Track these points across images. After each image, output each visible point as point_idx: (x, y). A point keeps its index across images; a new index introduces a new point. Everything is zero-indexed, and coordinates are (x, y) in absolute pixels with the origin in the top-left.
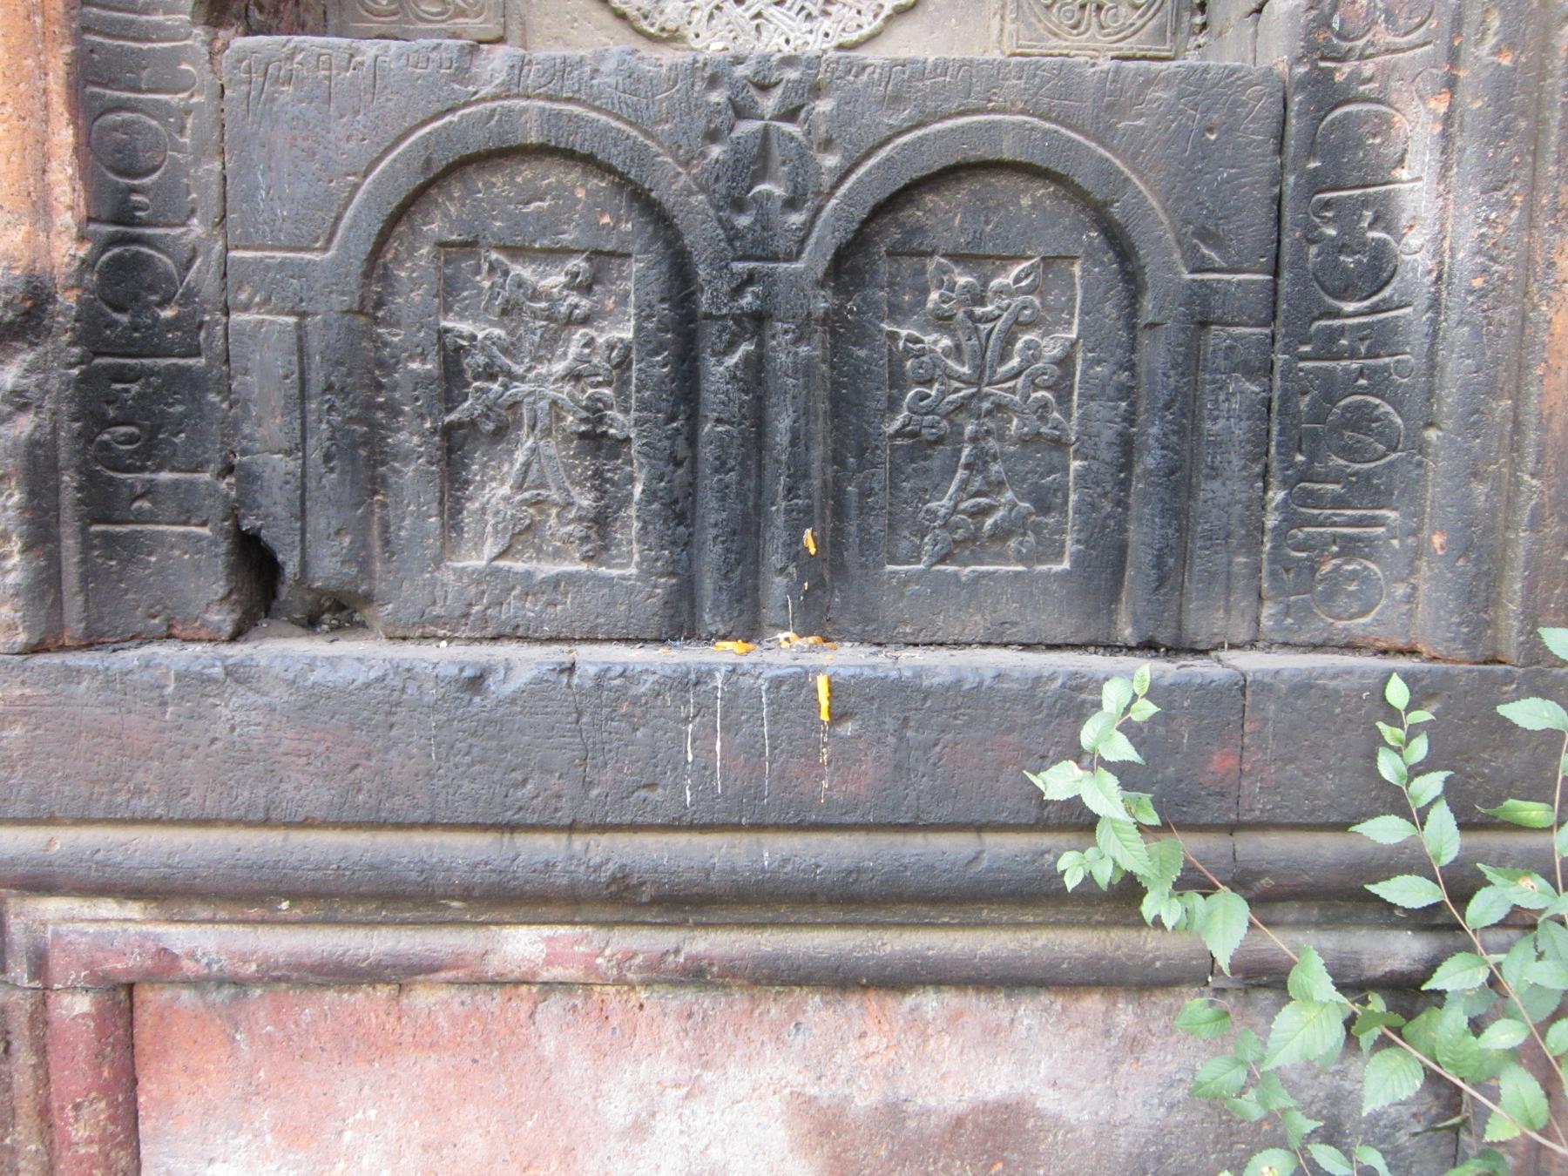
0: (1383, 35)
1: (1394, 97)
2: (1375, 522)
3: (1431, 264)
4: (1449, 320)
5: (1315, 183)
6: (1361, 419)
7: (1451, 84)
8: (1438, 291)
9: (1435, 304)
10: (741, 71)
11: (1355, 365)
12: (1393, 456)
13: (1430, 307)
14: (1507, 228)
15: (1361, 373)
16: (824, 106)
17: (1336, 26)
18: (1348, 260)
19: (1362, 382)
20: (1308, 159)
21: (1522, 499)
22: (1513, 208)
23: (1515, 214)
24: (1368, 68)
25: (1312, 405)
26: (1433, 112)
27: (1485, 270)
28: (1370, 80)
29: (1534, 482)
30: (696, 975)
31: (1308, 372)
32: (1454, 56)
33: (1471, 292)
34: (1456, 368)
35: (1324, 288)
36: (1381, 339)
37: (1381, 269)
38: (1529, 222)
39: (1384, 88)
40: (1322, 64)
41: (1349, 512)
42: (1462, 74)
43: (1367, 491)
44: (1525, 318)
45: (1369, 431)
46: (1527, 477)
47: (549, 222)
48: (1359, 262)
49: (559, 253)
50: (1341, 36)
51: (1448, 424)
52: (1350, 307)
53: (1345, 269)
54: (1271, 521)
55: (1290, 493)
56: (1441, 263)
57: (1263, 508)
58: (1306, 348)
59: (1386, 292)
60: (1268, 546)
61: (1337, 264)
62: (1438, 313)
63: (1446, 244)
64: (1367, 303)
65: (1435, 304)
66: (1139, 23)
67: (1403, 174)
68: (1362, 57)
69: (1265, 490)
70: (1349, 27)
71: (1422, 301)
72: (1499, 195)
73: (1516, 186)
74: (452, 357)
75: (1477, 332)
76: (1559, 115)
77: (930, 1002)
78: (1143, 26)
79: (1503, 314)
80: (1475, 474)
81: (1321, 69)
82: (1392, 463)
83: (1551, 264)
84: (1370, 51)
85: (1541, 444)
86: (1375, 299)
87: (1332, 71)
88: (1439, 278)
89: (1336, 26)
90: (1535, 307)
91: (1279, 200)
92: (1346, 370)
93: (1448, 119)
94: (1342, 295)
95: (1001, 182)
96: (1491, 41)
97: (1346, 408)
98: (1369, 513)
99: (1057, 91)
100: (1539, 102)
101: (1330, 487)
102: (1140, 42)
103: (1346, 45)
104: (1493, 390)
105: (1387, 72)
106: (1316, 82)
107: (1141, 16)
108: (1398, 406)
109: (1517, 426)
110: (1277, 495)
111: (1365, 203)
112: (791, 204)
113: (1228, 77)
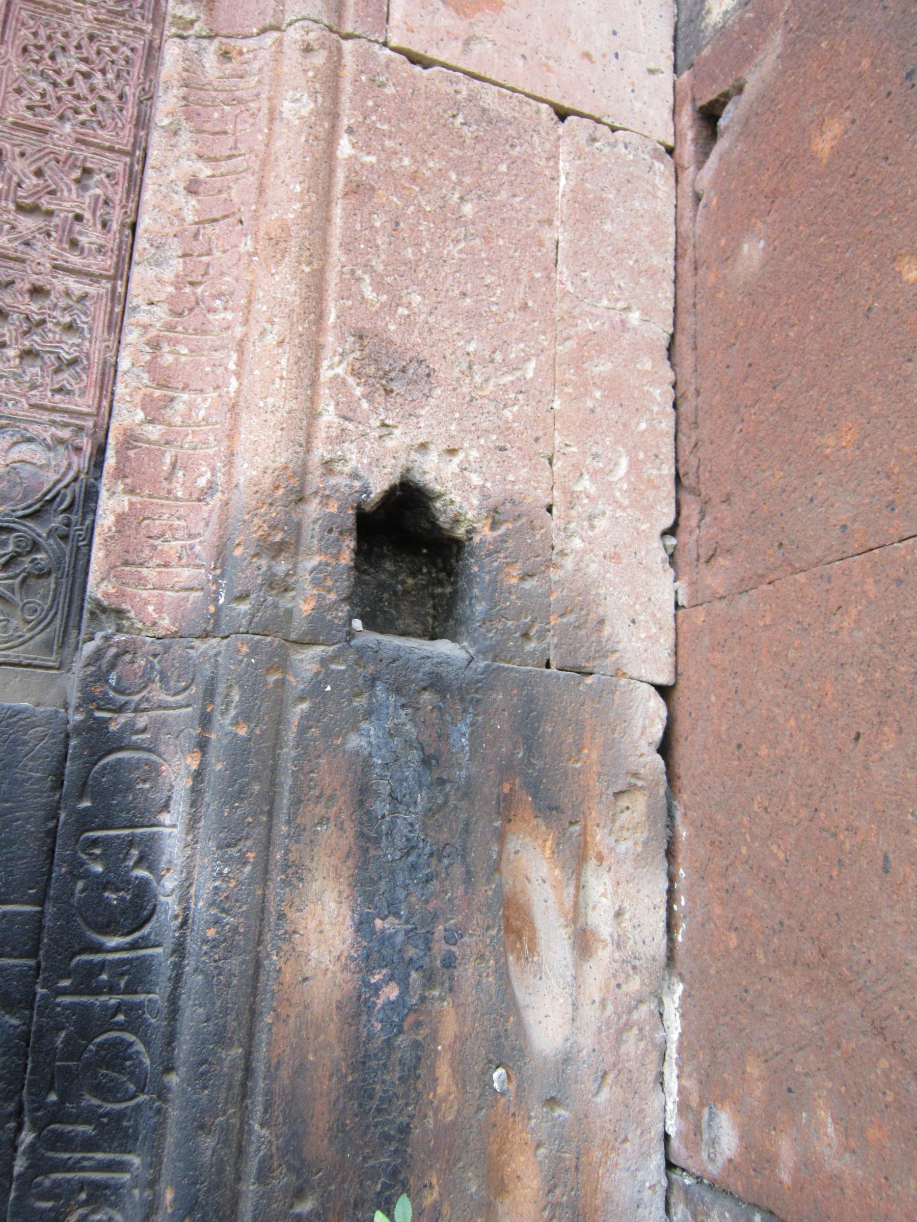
0: (157, 694)
1: (162, 748)
2: (121, 1167)
3: (177, 909)
4: (190, 965)
5: (85, 821)
6: (117, 1055)
7: (202, 745)
8: (183, 936)
9: (180, 949)
11: (114, 1000)
12: (142, 1098)
13: (174, 952)
14: (239, 883)
15: (118, 1009)
17: (113, 682)
18: (112, 896)
19: (121, 1017)
20: (81, 797)
21: (253, 1148)
22: (245, 864)
23: (247, 869)
24: (142, 721)
25: (66, 1042)
26: (187, 767)
27: (217, 922)
28: (144, 730)
29: (264, 1132)
31: (66, 1007)
32: (206, 720)
33: (205, 941)
34: (192, 1014)
35: (88, 923)
36: (137, 975)
37: (143, 908)
38: (264, 873)
39: (155, 739)
40: (98, 714)
41: (100, 1156)
42: (213, 736)
43: (116, 1133)
44: (258, 965)
45: (122, 1070)
46: (257, 1127)
48: (122, 899)
50: (115, 689)
51: (182, 1070)
52: (113, 941)
53: (109, 905)
54: (19, 1165)
55: (38, 1137)
56: (186, 909)
57: (15, 1149)
58: (65, 983)
59: (145, 930)
60: (12, 1195)
61: (101, 900)
62: (183, 958)
63: (192, 891)
64: (129, 939)
65: (180, 949)
66: (28, 635)
67: (166, 818)
68: (136, 710)
69: (19, 1129)
70: (125, 684)
71: (169, 944)
72: (233, 851)
73: (249, 843)
75: (208, 983)
76: (290, 782)
78: (31, 638)
79: (234, 964)
80: (202, 1127)
81: (97, 719)
82: (138, 1106)
83: (282, 916)
84: (145, 705)
85: (269, 1093)
86: (137, 935)
87: (107, 721)
88: (184, 923)
89: (113, 682)
90: (268, 956)
91: (52, 834)
92: (104, 1006)
93: (198, 775)
94: (107, 928)
96: (233, 712)
97: (101, 1045)
98: (117, 1157)
100: (274, 769)
101: (81, 1128)
102: (26, 651)
103: (122, 699)
104: (222, 1039)
106: (90, 729)
107: (31, 630)
108: (147, 1044)
109: (248, 1071)
110: (27, 1137)
113: (10, 717)
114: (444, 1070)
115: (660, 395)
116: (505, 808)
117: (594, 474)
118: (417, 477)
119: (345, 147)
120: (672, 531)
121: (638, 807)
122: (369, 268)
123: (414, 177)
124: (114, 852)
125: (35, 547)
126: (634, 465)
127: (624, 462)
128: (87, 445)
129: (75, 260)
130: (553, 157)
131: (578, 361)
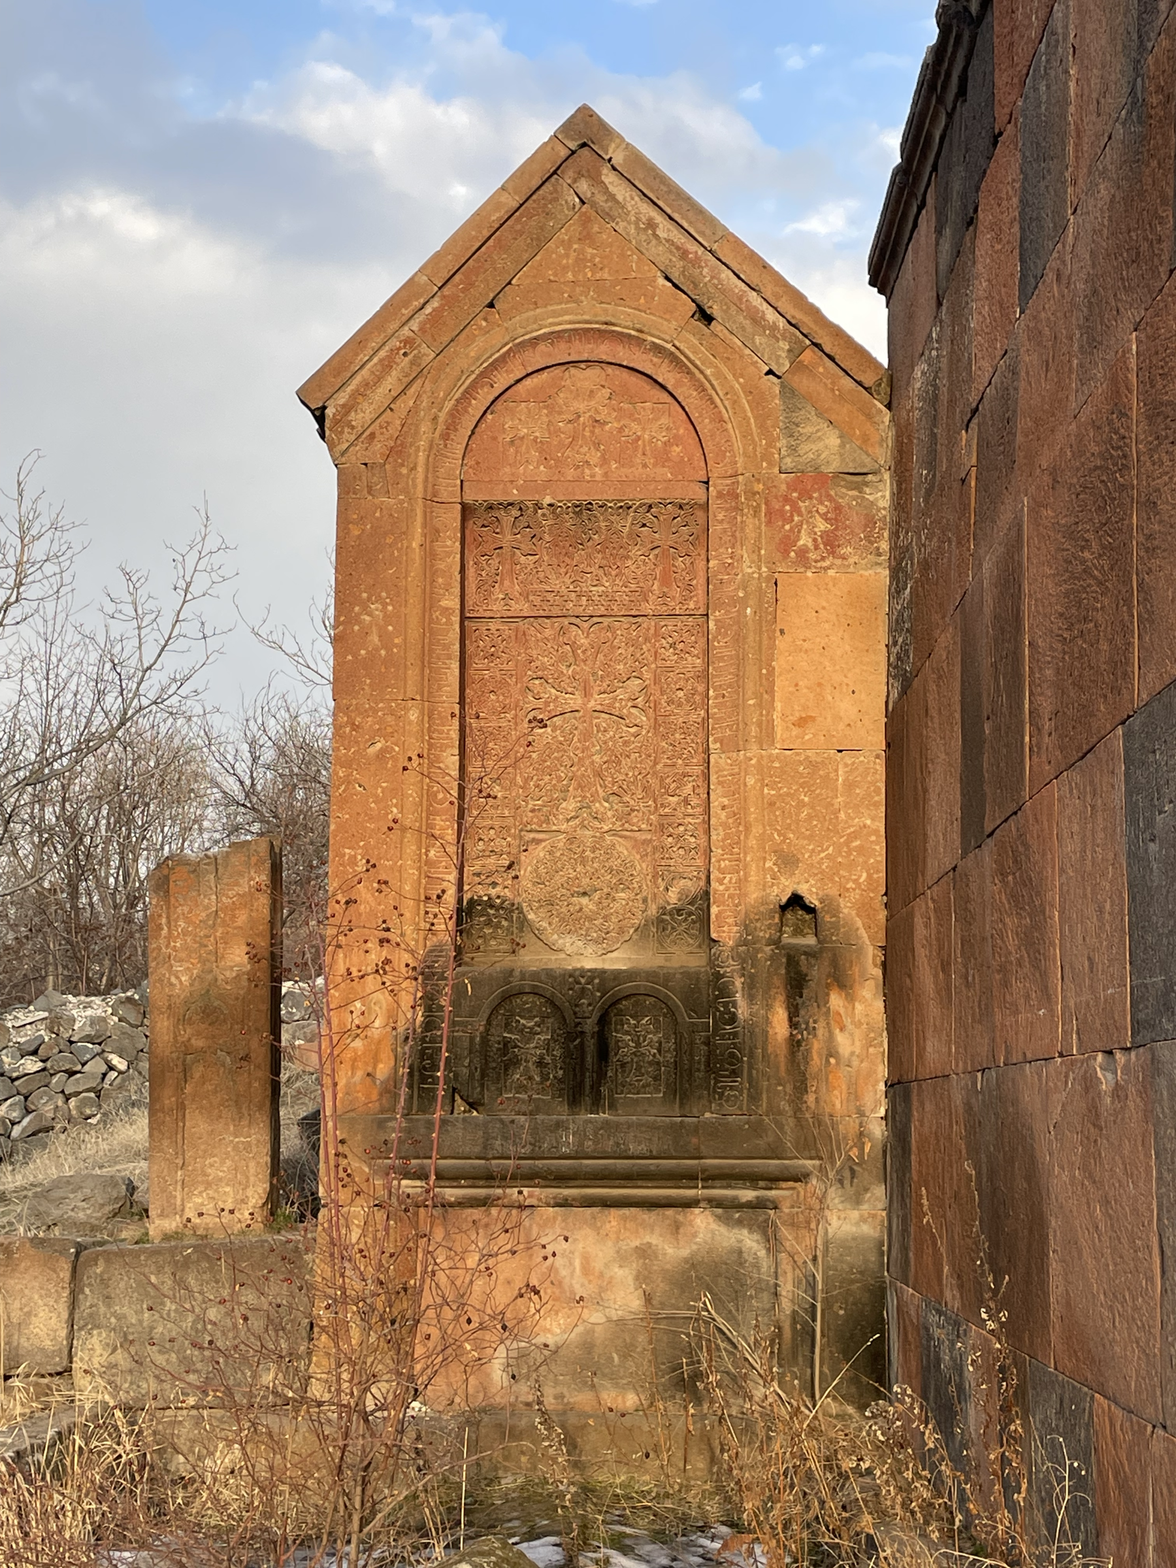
5: (717, 997)
6: (732, 1055)
10: (577, 973)
16: (597, 981)
30: (564, 1203)
36: (735, 1035)
43: (734, 1073)
47: (529, 1010)
49: (531, 1018)
74: (506, 1043)
77: (626, 1211)
95: (641, 998)
99: (652, 976)
105: (733, 971)
111: (728, 1002)
112: (590, 1005)
114: (815, 1056)
115: (880, 848)
116: (828, 986)
117: (855, 881)
118: (799, 892)
119: (766, 791)
120: (886, 894)
121: (870, 984)
122: (776, 830)
123: (788, 794)
124: (726, 1005)
125: (690, 914)
126: (869, 876)
127: (864, 875)
128: (704, 878)
129: (690, 811)
130: (836, 771)
131: (847, 843)
